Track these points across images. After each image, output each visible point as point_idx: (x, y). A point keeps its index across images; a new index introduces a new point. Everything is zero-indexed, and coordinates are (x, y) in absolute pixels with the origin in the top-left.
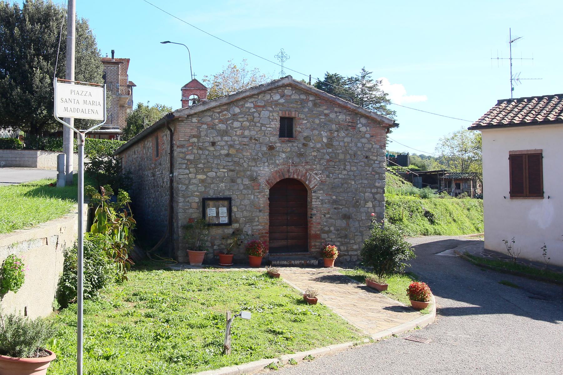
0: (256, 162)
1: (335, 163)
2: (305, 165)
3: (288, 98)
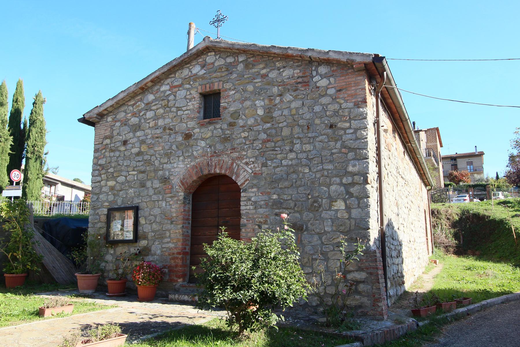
0: (169, 158)
1: (275, 143)
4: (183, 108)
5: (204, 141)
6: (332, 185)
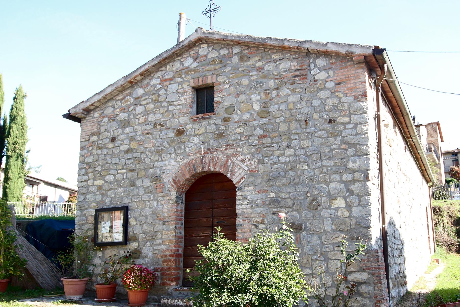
0: (160, 155)
1: (272, 139)
2: (226, 149)
3: (204, 58)
4: (174, 103)
5: (196, 137)
6: (331, 182)
